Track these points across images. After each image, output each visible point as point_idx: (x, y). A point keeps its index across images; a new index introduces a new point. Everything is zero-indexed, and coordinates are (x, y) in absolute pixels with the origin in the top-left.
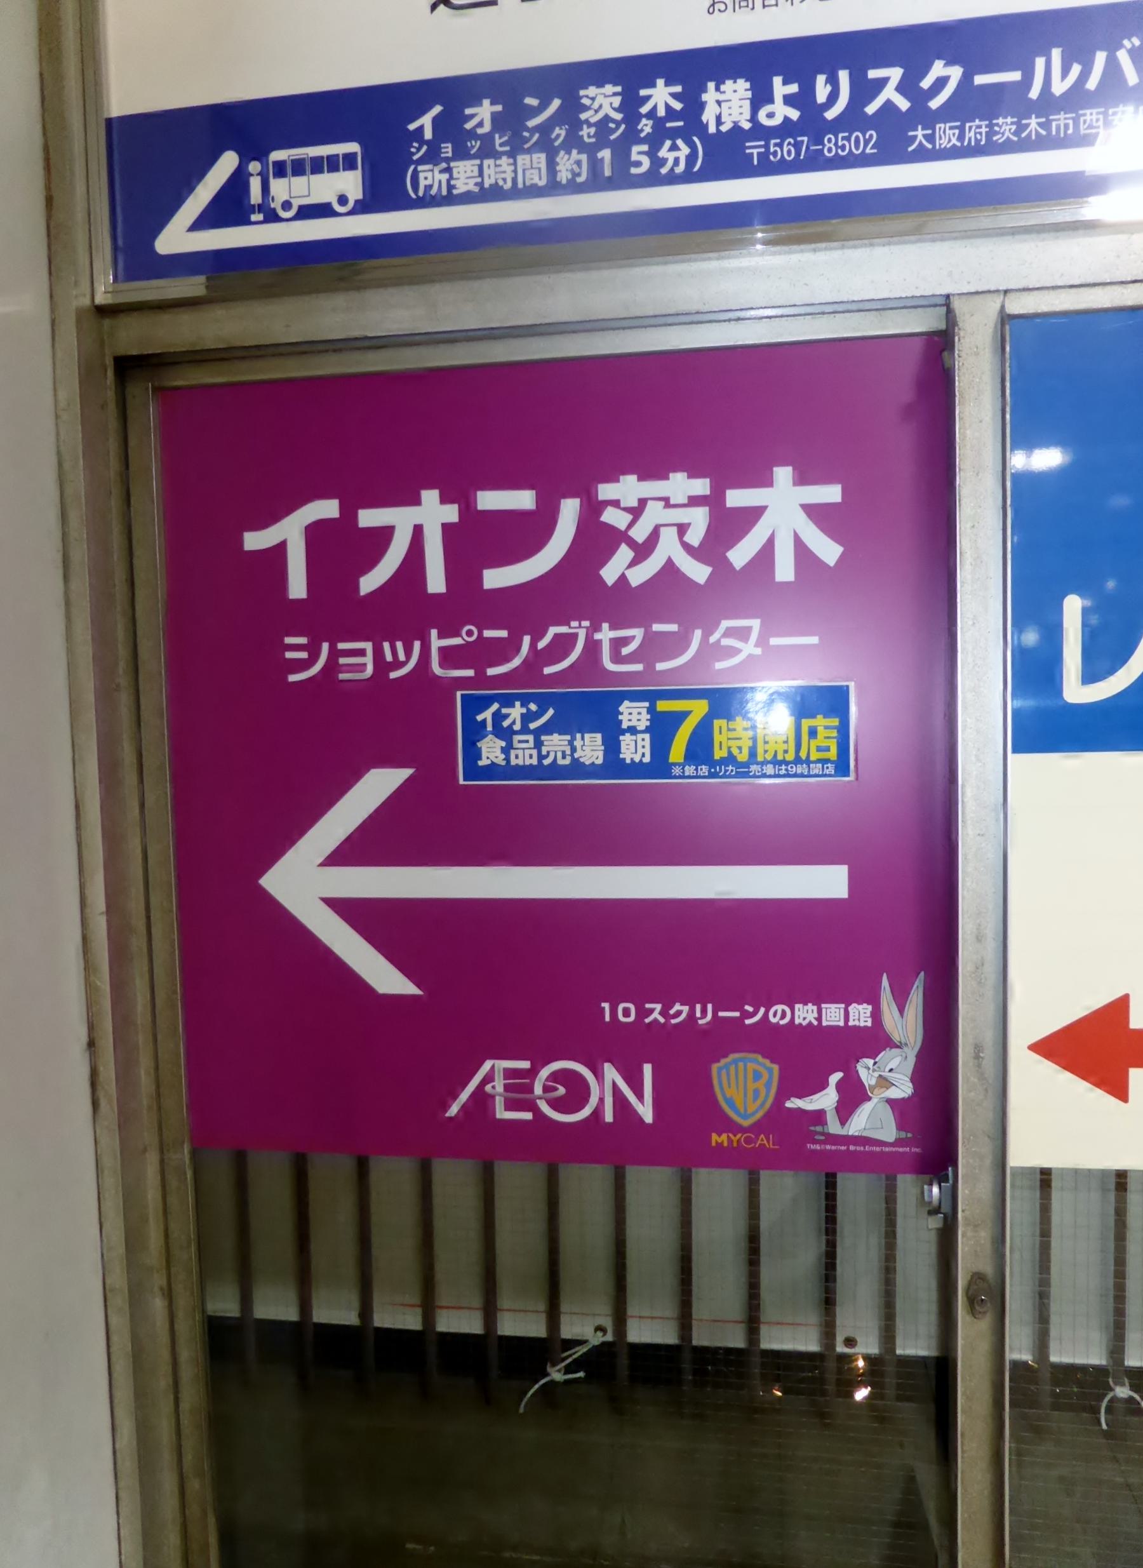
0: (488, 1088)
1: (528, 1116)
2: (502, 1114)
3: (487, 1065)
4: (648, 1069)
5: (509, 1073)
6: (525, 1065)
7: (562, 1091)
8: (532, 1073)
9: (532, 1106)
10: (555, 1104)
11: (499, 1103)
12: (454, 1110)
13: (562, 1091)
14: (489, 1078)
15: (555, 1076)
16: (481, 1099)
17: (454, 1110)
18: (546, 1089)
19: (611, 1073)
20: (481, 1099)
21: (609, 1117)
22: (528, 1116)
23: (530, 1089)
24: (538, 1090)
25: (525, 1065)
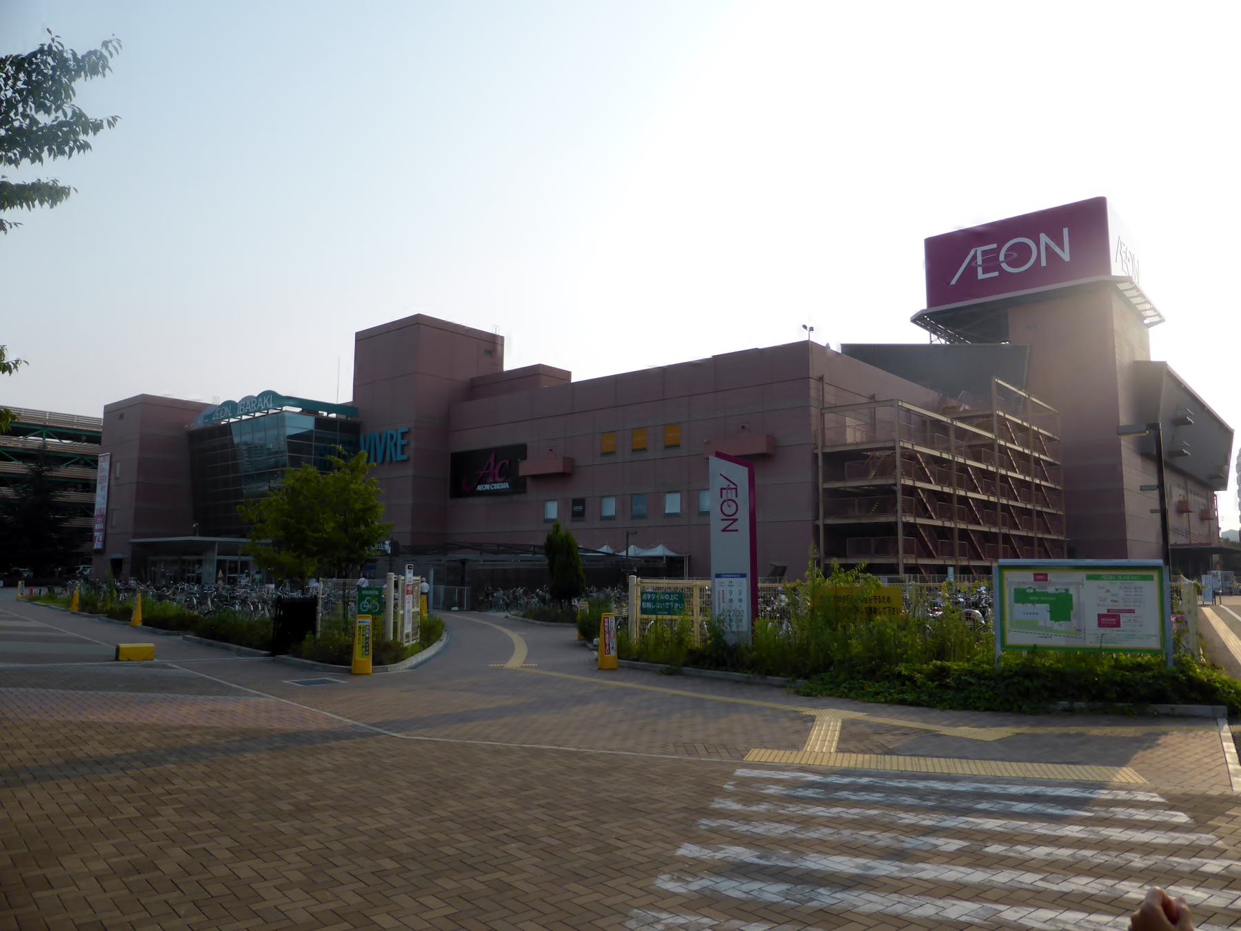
0: (973, 264)
1: (996, 274)
2: (981, 276)
3: (972, 253)
4: (1066, 231)
5: (984, 253)
6: (994, 246)
7: (1015, 255)
8: (998, 251)
10: (1010, 264)
11: (980, 270)
12: (953, 282)
14: (975, 257)
15: (1009, 249)
16: (971, 270)
17: (953, 282)
18: (1006, 256)
19: (1044, 238)
20: (971, 270)
21: (1044, 263)
22: (996, 274)
23: (997, 258)
24: (1002, 257)
25: (994, 246)
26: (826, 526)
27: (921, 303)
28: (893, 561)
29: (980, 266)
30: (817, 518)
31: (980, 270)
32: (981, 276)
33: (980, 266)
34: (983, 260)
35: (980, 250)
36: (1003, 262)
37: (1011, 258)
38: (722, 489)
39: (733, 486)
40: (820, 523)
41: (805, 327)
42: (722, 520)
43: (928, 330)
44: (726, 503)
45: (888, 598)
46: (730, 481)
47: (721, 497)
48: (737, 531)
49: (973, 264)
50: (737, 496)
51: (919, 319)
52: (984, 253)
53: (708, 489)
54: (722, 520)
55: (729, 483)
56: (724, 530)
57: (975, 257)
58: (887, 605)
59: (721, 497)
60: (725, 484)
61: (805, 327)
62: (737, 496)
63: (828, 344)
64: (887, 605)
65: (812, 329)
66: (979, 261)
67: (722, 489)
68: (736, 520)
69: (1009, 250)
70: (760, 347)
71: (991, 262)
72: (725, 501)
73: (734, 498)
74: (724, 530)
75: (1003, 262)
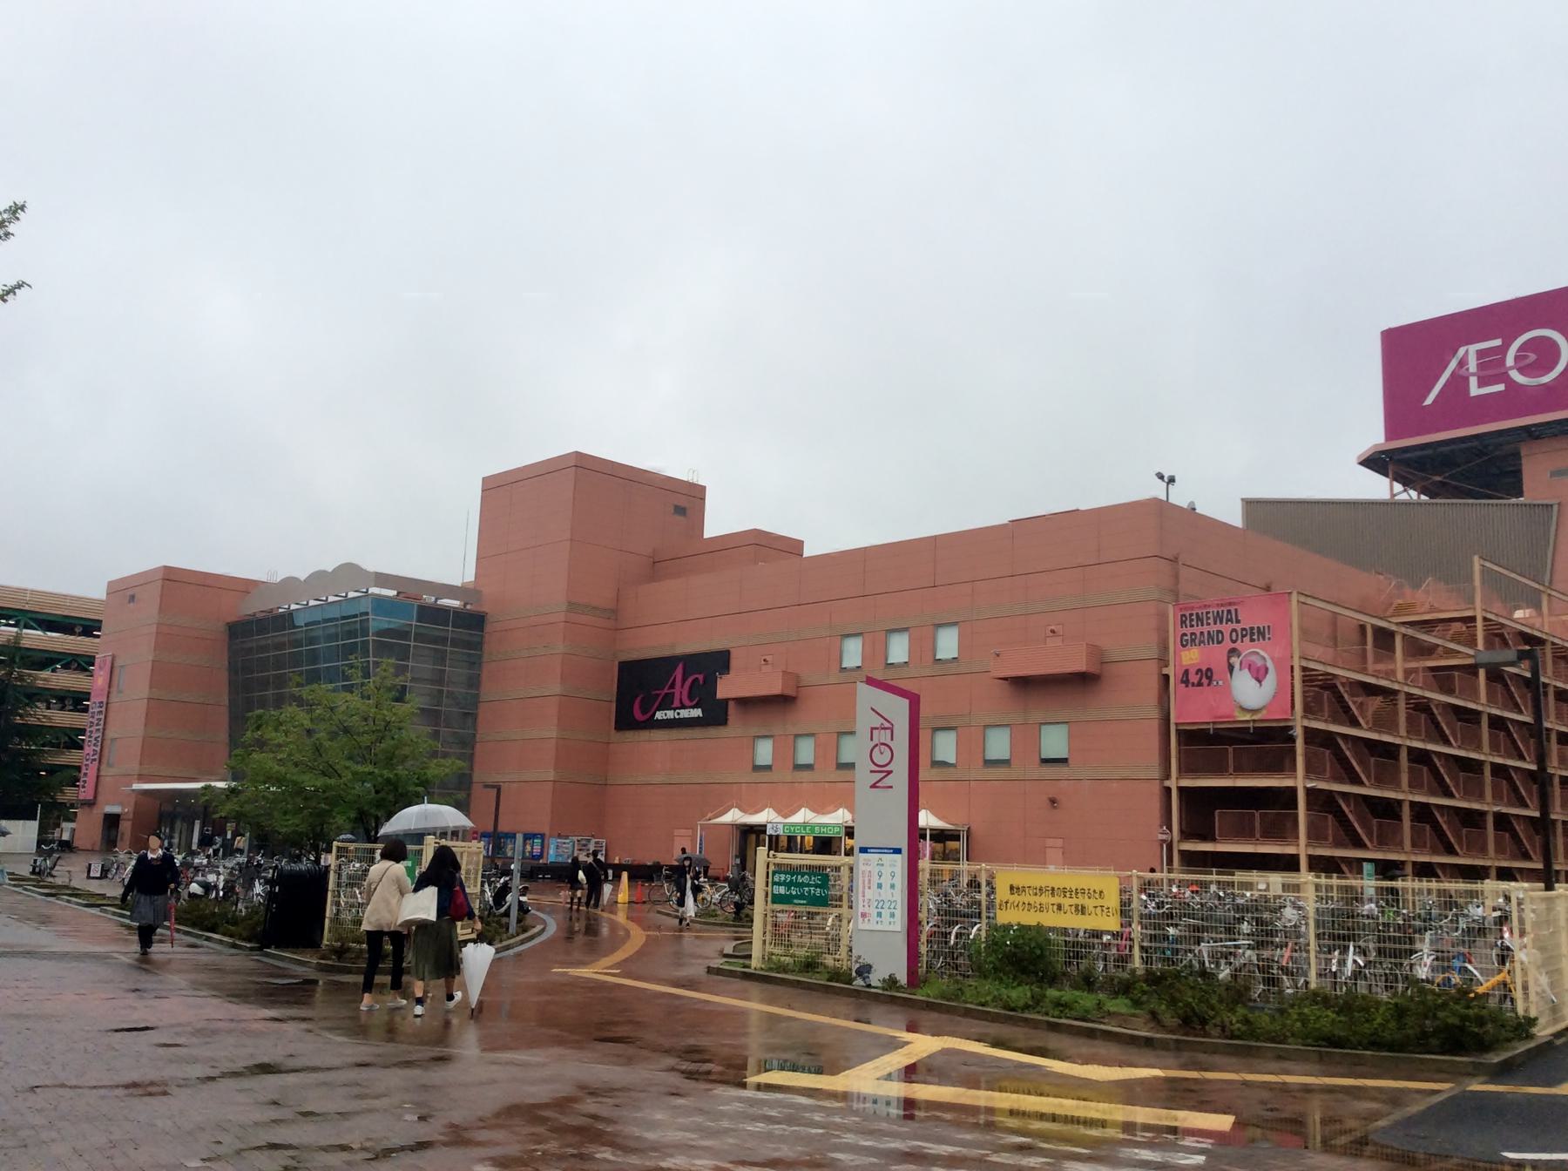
1: (1500, 387)
2: (1475, 390)
3: (1462, 351)
5: (1481, 354)
6: (1497, 342)
7: (1532, 357)
8: (1503, 350)
9: (1504, 377)
10: (1522, 371)
11: (1473, 381)
12: (1429, 401)
13: (1532, 357)
15: (1522, 348)
16: (1459, 381)
17: (1429, 401)
18: (1517, 358)
20: (1459, 381)
22: (1500, 387)
23: (1503, 360)
24: (1510, 361)
25: (1497, 342)
26: (1181, 789)
27: (1374, 435)
28: (1290, 850)
29: (1473, 374)
30: (1168, 777)
31: (1473, 381)
32: (1475, 390)
33: (1473, 374)
34: (1478, 365)
35: (1473, 349)
36: (1511, 368)
37: (1522, 364)
38: (872, 729)
39: (887, 725)
40: (1172, 784)
41: (1161, 477)
42: (872, 772)
43: (1386, 475)
44: (876, 749)
45: (1101, 892)
46: (886, 720)
47: (872, 739)
48: (891, 787)
49: (1463, 372)
50: (892, 739)
51: (1375, 462)
52: (1481, 354)
53: (852, 733)
54: (872, 772)
55: (884, 722)
56: (874, 786)
57: (1462, 363)
58: (1100, 902)
59: (872, 739)
60: (878, 722)
61: (1161, 477)
62: (892, 739)
63: (1192, 503)
64: (1100, 902)
65: (1172, 480)
66: (1472, 366)
67: (872, 729)
68: (889, 773)
69: (1518, 350)
70: (1084, 506)
71: (1491, 367)
72: (876, 745)
73: (888, 742)
74: (874, 786)
75: (1511, 368)
